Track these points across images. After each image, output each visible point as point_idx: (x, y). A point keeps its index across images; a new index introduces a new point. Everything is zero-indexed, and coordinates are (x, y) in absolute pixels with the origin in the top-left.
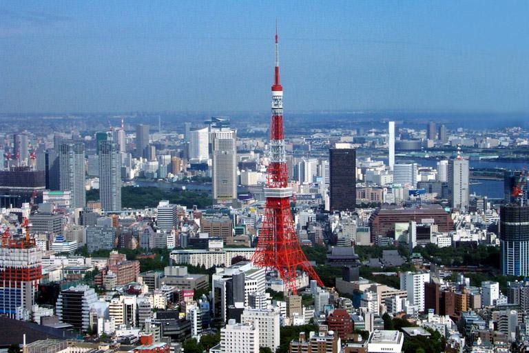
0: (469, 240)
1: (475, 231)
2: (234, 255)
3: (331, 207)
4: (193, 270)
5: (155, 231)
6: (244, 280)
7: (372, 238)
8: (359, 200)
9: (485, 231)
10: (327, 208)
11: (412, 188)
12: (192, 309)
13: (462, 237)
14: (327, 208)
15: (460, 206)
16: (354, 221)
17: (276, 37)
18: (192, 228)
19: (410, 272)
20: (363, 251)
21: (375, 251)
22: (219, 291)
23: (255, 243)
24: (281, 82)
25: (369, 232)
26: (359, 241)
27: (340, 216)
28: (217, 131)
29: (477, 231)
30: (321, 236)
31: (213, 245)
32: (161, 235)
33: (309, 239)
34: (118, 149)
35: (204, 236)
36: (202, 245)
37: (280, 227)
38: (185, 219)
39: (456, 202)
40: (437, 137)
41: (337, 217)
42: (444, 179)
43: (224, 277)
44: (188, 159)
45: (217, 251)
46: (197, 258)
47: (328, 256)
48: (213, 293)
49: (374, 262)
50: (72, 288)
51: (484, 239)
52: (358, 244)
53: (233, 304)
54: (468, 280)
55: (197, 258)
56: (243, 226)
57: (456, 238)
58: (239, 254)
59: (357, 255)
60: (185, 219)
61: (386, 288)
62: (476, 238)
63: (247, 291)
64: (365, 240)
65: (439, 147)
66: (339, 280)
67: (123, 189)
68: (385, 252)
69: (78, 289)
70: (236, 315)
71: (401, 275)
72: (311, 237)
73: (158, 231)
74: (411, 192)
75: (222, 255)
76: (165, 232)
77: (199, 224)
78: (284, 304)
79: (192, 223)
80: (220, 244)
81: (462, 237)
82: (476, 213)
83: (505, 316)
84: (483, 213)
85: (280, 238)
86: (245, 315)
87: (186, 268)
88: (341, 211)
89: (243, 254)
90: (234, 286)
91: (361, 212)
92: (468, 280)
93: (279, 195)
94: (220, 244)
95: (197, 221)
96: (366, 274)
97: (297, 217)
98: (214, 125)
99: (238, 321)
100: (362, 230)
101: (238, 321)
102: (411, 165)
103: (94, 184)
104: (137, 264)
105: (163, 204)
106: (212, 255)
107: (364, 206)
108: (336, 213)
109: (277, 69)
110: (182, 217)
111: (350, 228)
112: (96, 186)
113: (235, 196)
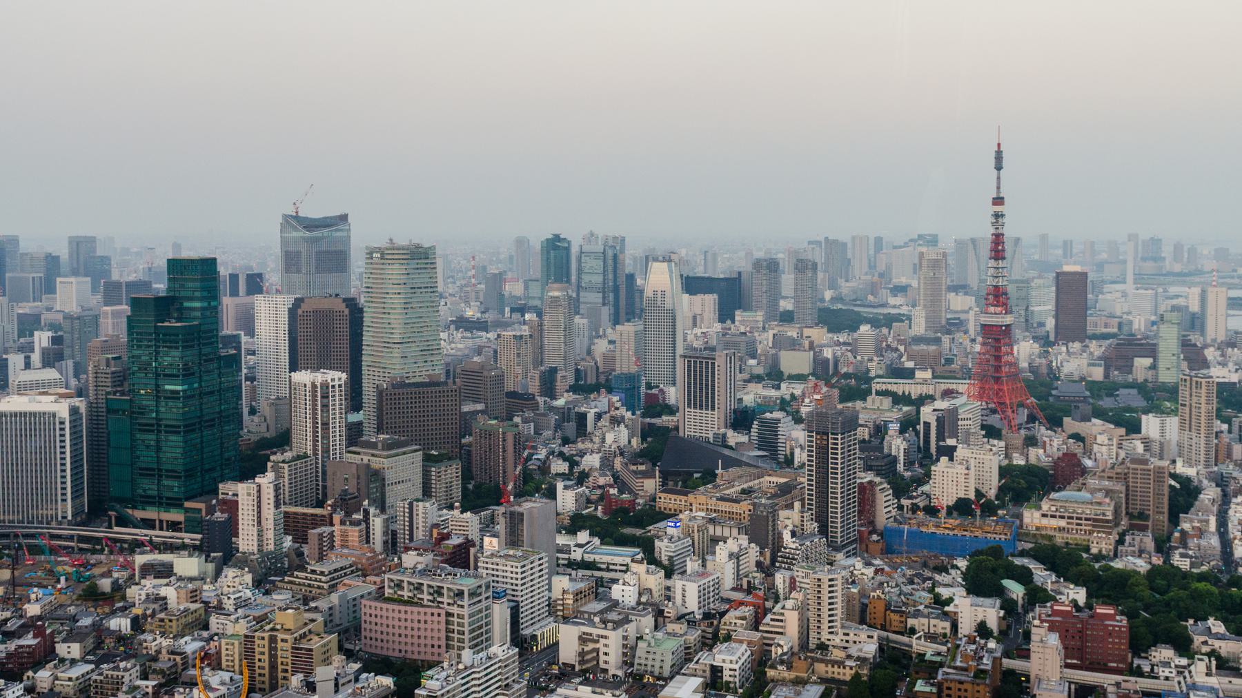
2: (943, 387)
3: (1056, 337)
4: (898, 399)
7: (1107, 376)
8: (1090, 330)
10: (1052, 338)
11: (1153, 318)
12: (897, 445)
14: (1052, 338)
15: (1214, 340)
18: (895, 355)
20: (1094, 387)
21: (1108, 388)
22: (927, 425)
23: (966, 374)
28: (924, 249)
30: (1044, 370)
32: (861, 362)
34: (815, 266)
35: (910, 365)
36: (909, 374)
37: (998, 358)
38: (888, 346)
39: (1210, 333)
41: (1064, 349)
42: (1195, 307)
45: (924, 382)
46: (901, 386)
47: (1054, 392)
48: (921, 428)
49: (1106, 403)
50: (768, 415)
59: (1088, 393)
60: (888, 346)
61: (1122, 431)
64: (1098, 374)
66: (1067, 420)
67: (820, 310)
68: (1122, 391)
69: (777, 415)
71: (1144, 417)
72: (1033, 369)
73: (859, 358)
74: (1154, 323)
78: (1002, 444)
79: (897, 350)
80: (928, 375)
85: (998, 369)
86: (961, 452)
89: (954, 386)
90: (947, 423)
92: (1225, 427)
94: (928, 375)
95: (902, 348)
96: (1100, 414)
97: (1015, 348)
99: (951, 459)
100: (1094, 365)
101: (951, 459)
103: (786, 305)
104: (836, 392)
105: (864, 328)
107: (1095, 337)
111: (1077, 363)
112: (790, 307)
113: (944, 323)
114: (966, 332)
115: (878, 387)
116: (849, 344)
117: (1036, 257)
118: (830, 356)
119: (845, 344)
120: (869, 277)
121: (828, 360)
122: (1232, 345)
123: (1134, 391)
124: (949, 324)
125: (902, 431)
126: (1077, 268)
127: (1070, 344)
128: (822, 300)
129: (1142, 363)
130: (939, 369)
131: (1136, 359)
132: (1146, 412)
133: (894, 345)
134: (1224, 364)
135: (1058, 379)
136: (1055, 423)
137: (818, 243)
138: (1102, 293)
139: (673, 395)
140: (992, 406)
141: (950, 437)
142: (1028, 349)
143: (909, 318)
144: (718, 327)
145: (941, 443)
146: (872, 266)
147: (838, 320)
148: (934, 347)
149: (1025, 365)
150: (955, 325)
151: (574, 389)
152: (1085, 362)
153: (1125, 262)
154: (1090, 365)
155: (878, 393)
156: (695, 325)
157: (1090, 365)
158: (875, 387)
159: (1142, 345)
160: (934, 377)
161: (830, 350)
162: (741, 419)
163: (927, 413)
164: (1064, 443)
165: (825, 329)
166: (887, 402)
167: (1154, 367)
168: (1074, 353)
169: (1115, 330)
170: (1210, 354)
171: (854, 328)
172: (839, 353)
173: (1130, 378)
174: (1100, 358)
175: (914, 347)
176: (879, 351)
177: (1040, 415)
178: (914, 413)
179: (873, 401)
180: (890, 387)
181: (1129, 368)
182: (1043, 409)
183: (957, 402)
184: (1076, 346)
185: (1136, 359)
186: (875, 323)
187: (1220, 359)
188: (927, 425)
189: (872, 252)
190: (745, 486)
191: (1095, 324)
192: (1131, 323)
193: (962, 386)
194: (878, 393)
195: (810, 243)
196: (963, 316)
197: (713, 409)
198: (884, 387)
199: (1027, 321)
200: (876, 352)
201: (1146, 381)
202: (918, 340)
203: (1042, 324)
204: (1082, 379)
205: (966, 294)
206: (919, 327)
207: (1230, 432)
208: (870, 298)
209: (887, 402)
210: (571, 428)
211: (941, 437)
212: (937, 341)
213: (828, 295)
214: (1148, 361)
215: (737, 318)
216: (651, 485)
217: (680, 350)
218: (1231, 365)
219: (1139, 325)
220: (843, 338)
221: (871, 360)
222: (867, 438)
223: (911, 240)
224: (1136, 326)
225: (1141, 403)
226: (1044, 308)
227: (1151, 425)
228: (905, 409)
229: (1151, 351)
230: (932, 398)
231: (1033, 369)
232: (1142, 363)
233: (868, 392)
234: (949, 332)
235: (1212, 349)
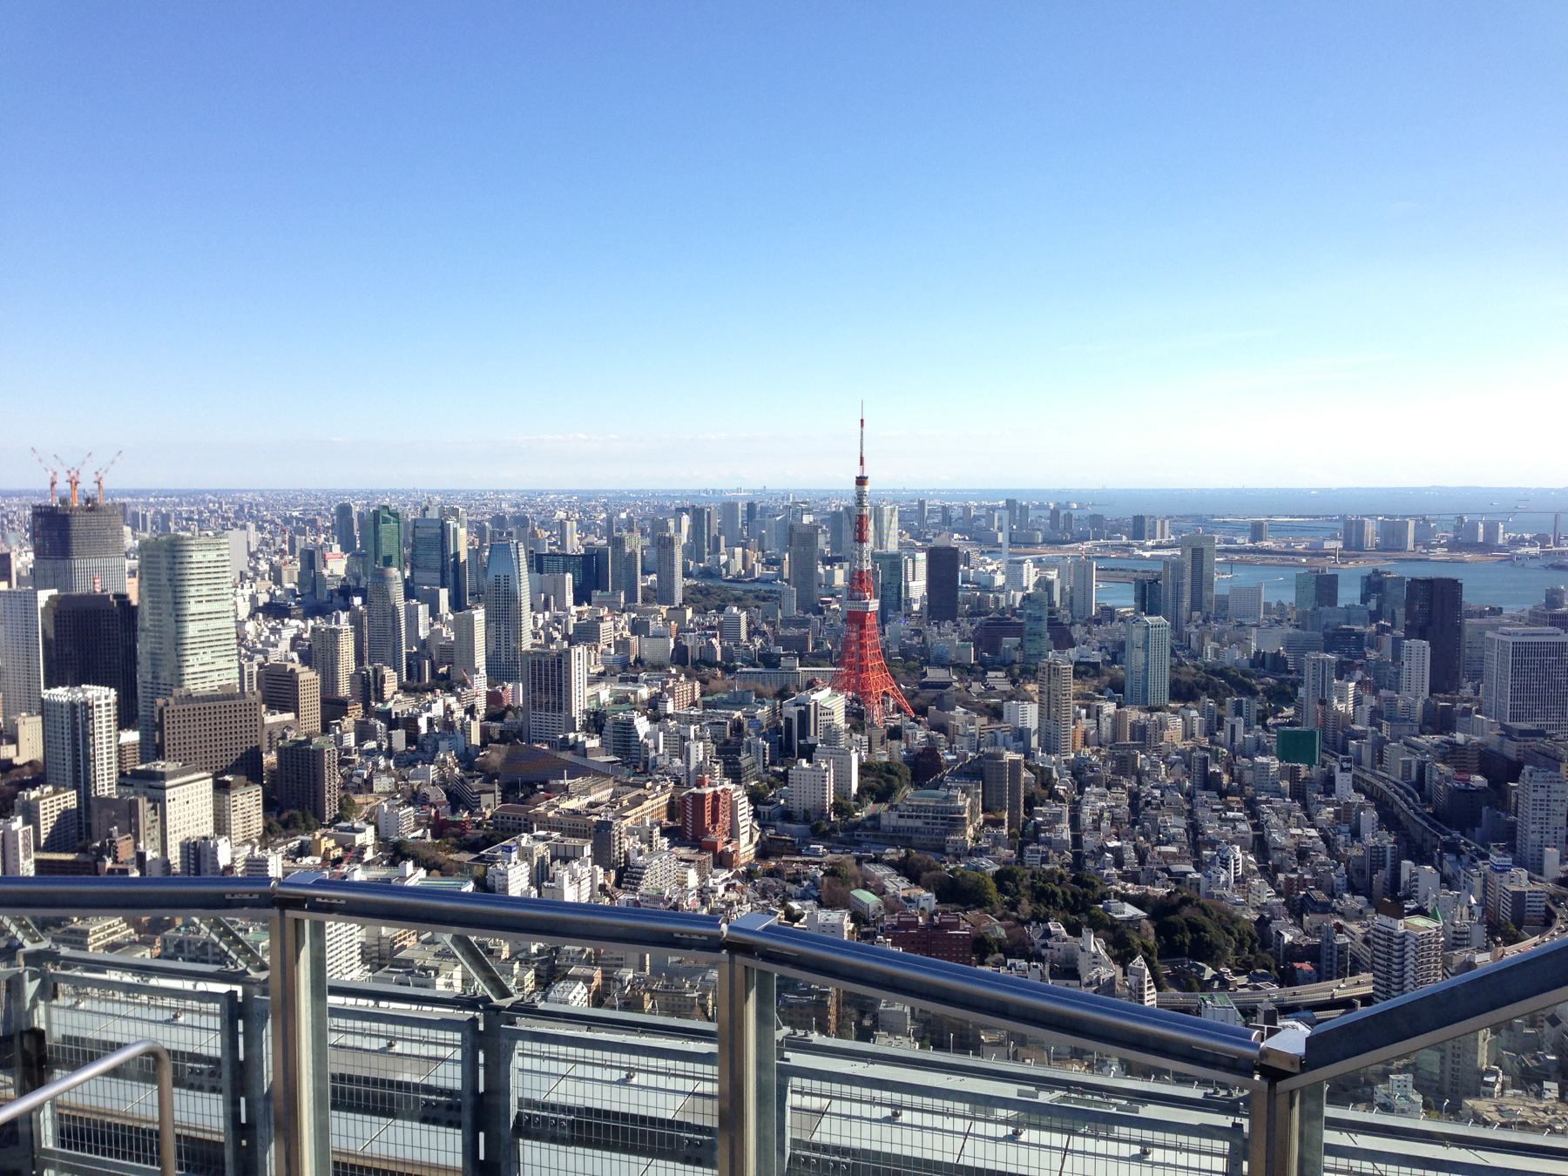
35: (780, 649)
49: (977, 687)
68: (990, 674)
70: (808, 752)
122: (1098, 622)
136: (921, 711)
137: (686, 510)
139: (515, 693)
144: (574, 610)
151: (404, 688)
156: (547, 607)
162: (596, 722)
167: (1021, 646)
170: (1078, 632)
171: (721, 609)
184: (948, 624)
188: (789, 721)
190: (591, 799)
197: (560, 709)
202: (787, 622)
210: (399, 737)
215: (594, 599)
216: (490, 804)
217: (527, 643)
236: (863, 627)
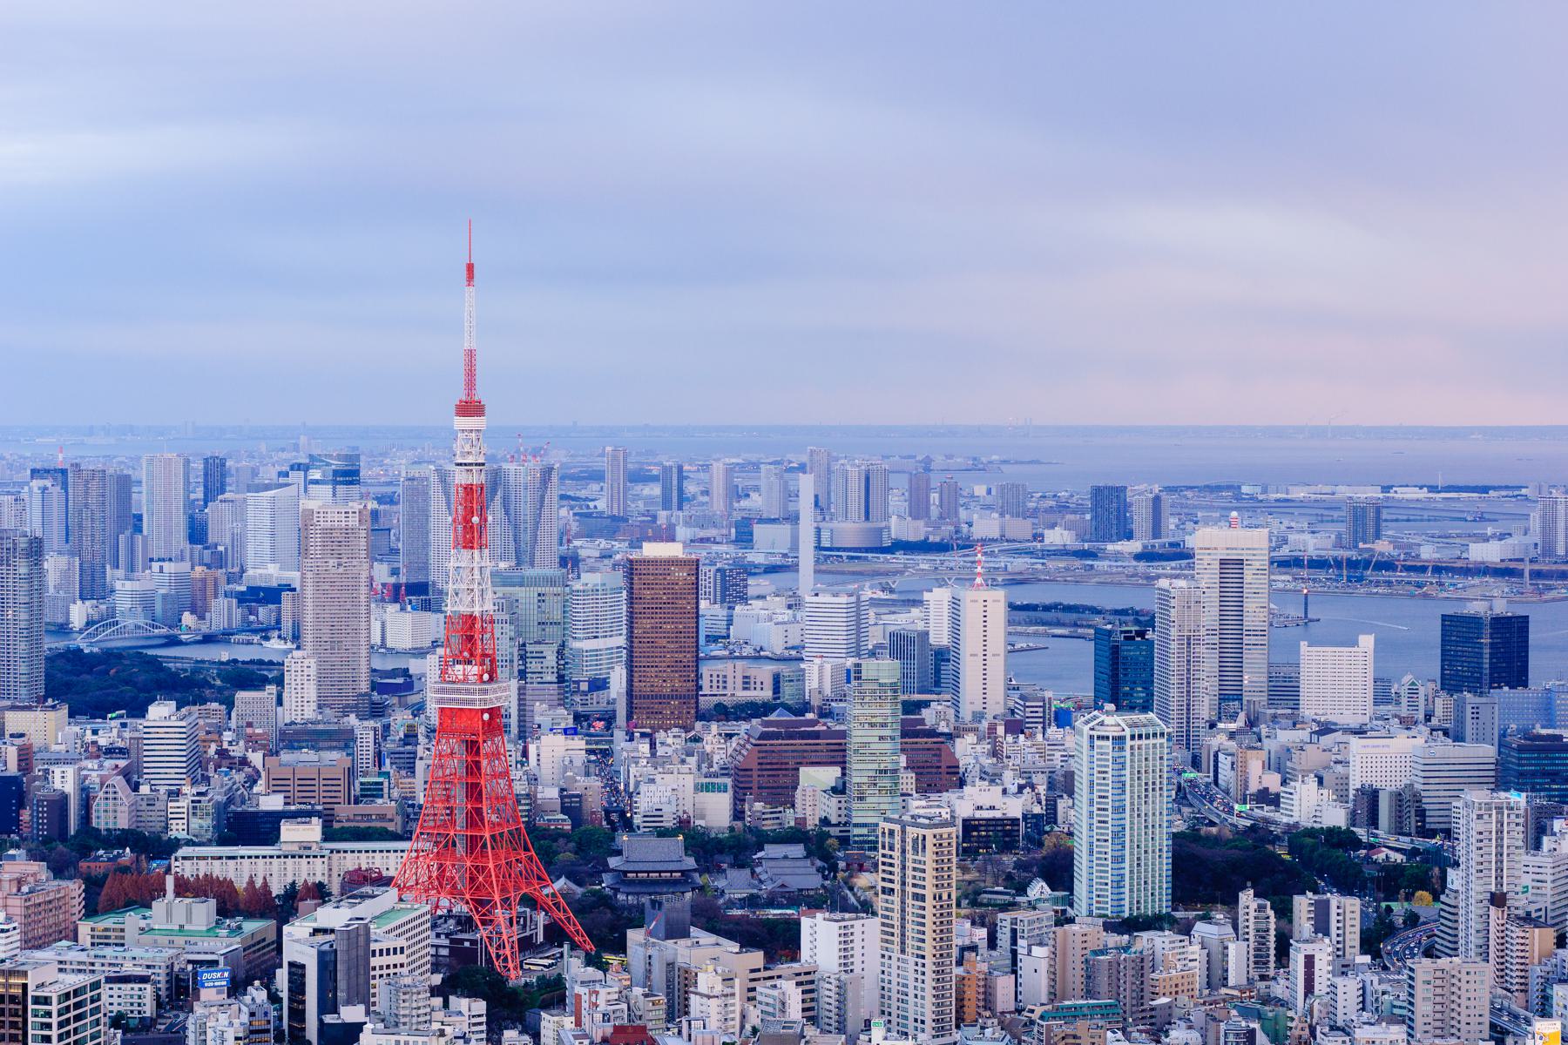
0: (998, 814)
1: (1014, 789)
2: (350, 863)
5: (136, 788)
6: (368, 941)
7: (738, 815)
9: (1042, 789)
13: (980, 808)
16: (689, 759)
17: (470, 268)
18: (239, 777)
19: (827, 915)
20: (709, 850)
21: (738, 848)
22: (297, 970)
24: (480, 394)
25: (730, 791)
26: (703, 817)
27: (653, 745)
29: (1021, 788)
31: (290, 832)
33: (564, 810)
35: (273, 803)
37: (474, 792)
38: (222, 753)
40: (934, 511)
41: (645, 748)
43: (316, 931)
44: (243, 571)
45: (304, 851)
46: (245, 867)
48: (282, 977)
51: (1037, 810)
52: (698, 822)
53: (335, 1011)
54: (982, 933)
55: (245, 867)
56: (380, 774)
57: (965, 810)
58: (364, 862)
59: (690, 863)
60: (222, 753)
61: (757, 958)
62: (1014, 808)
63: (377, 973)
64: (716, 812)
65: (938, 539)
66: (634, 936)
68: (771, 850)
71: (805, 922)
72: (571, 805)
73: (145, 789)
75: (319, 860)
76: (163, 790)
77: (260, 767)
79: (244, 762)
81: (980, 808)
82: (1022, 737)
83: (1075, 1037)
84: (1039, 737)
85: (475, 817)
87: (213, 903)
88: (655, 729)
91: (712, 737)
92: (982, 933)
93: (472, 702)
95: (256, 758)
96: (711, 919)
97: (532, 749)
98: (316, 474)
102: (853, 599)
104: (74, 889)
105: (160, 712)
106: (289, 861)
107: (723, 713)
108: (643, 735)
109: (471, 354)
110: (213, 747)
111: (675, 784)
113: (364, 687)
114: (418, 709)
115: (188, 870)
116: (123, 752)
117: (601, 505)
118: (69, 787)
119: (111, 751)
120: (185, 566)
121: (64, 798)
123: (798, 850)
124: (374, 686)
125: (236, 988)
126: (673, 550)
127: (660, 736)
128: (63, 629)
129: (816, 777)
130: (345, 812)
131: (802, 769)
132: (815, 903)
133: (237, 751)
134: (993, 778)
135: (628, 825)
138: (744, 599)
140: (461, 908)
141: (349, 1002)
142: (560, 752)
143: (280, 681)
145: (329, 1019)
146: (197, 533)
147: (96, 683)
148: (335, 755)
149: (554, 793)
150: (395, 686)
152: (690, 781)
153: (793, 519)
154: (700, 788)
155: (183, 888)
157: (700, 788)
158: (187, 865)
159: (817, 735)
160: (329, 835)
161: (70, 771)
163: (299, 942)
164: (623, 997)
165: (65, 711)
166: (204, 911)
167: (839, 790)
168: (667, 759)
169: (767, 694)
170: (967, 751)
171: (139, 711)
172: (94, 777)
173: (789, 818)
174: (724, 771)
175: (285, 756)
176: (198, 769)
177: (574, 927)
178: (272, 937)
179: (168, 911)
180: (218, 870)
181: (783, 794)
182: (581, 908)
183: (366, 909)
184: (671, 741)
185: (802, 769)
186: (186, 688)
187: (988, 762)
188: (297, 970)
189: (199, 494)
191: (724, 680)
192: (801, 677)
193: (386, 858)
194: (183, 888)
195: (35, 473)
196: (414, 666)
198: (203, 868)
199: (561, 679)
200: (190, 772)
201: (825, 821)
202: (294, 738)
203: (599, 684)
204: (683, 825)
205: (427, 606)
206: (301, 701)
207: (992, 943)
208: (188, 619)
209: (204, 911)
211: (328, 1004)
212: (345, 740)
213: (78, 614)
214: (830, 775)
218: (1008, 776)
219: (818, 678)
220: (109, 732)
221: (175, 794)
222: (149, 1010)
223: (297, 467)
224: (812, 683)
225: (808, 878)
226: (602, 647)
227: (820, 936)
228: (251, 926)
229: (838, 755)
230: (320, 893)
231: (571, 805)
232: (816, 777)
233: (162, 891)
234: (377, 711)
235: (971, 738)
236: (473, 747)
